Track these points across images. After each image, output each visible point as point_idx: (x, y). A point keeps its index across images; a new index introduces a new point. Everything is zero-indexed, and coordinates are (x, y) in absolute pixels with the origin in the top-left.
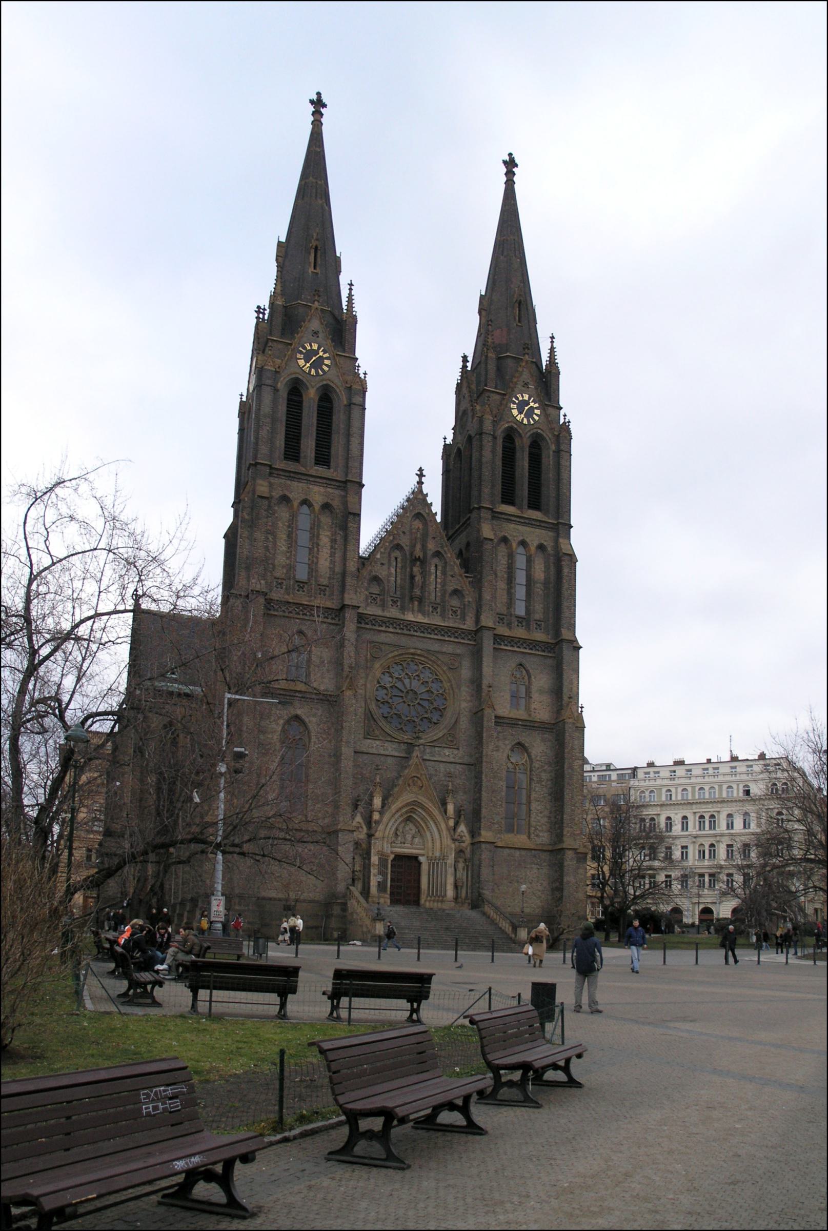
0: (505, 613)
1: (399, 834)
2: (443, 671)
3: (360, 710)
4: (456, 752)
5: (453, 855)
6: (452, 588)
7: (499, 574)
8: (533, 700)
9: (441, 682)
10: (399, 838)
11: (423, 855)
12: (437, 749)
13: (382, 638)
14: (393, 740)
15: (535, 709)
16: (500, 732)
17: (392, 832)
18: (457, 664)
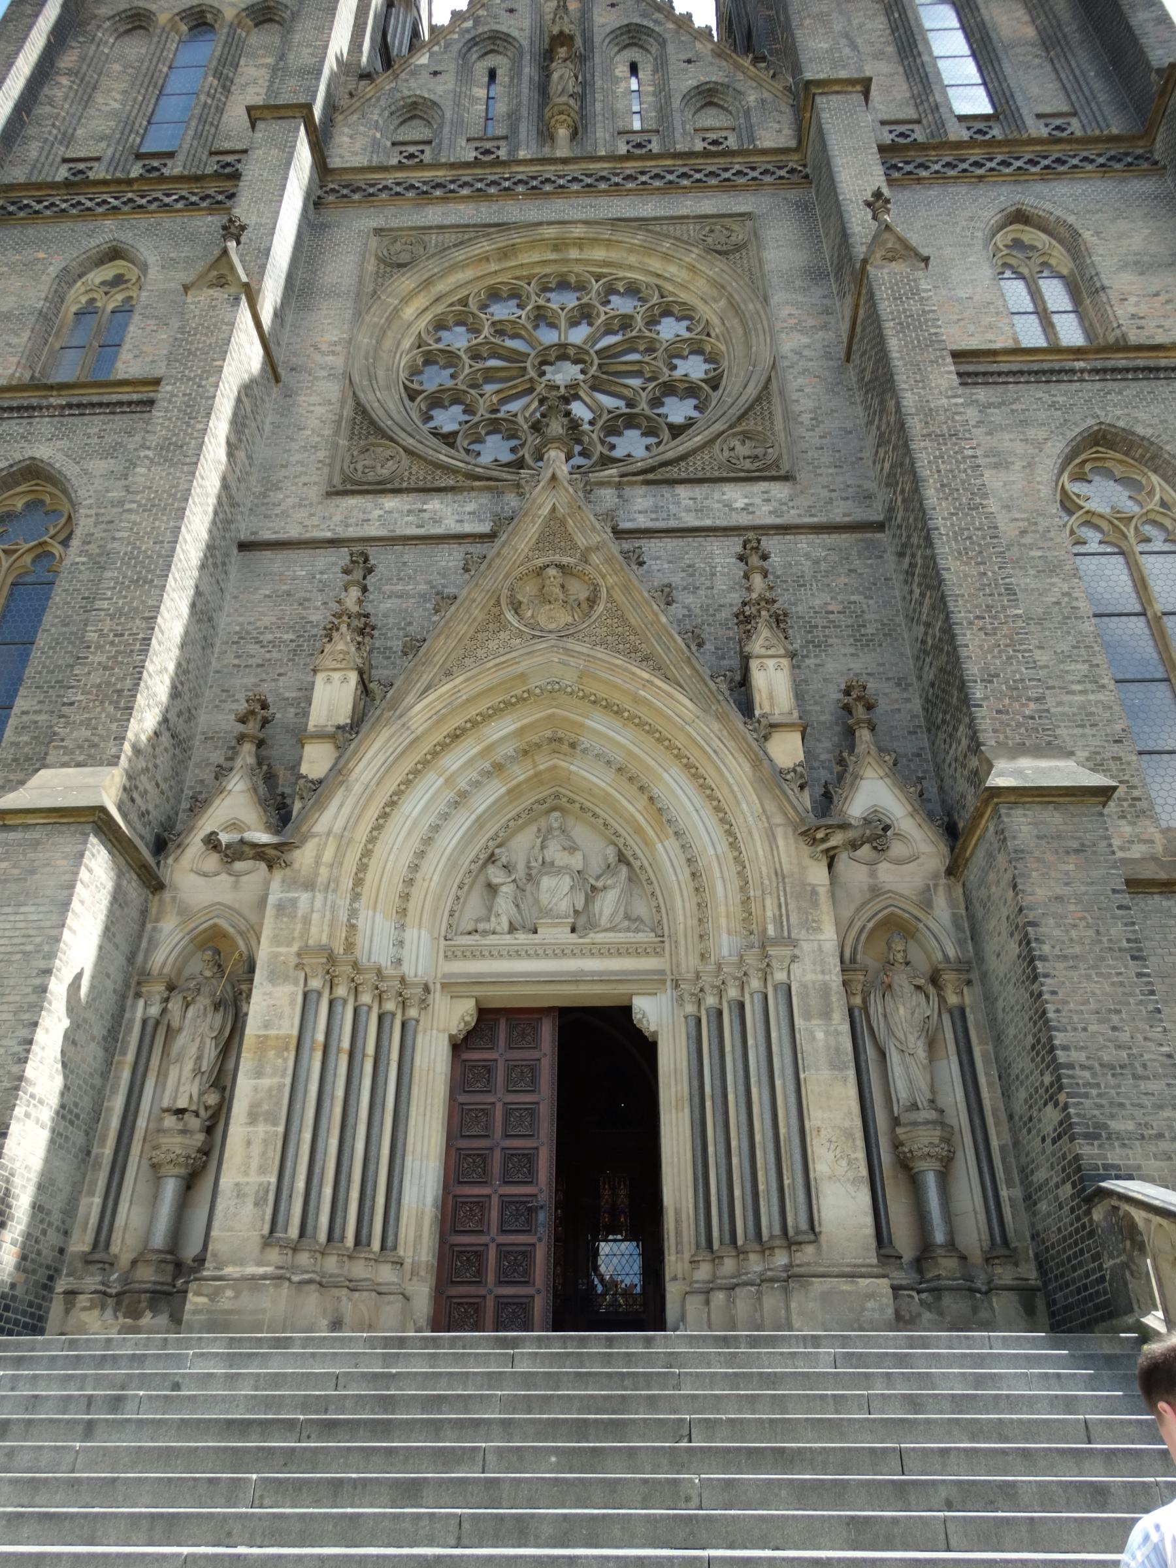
0: (915, 116)
1: (496, 875)
2: (692, 269)
3: (320, 410)
4: (779, 490)
5: (828, 936)
6: (692, 83)
7: (865, 49)
8: (1114, 296)
9: (686, 314)
10: (504, 904)
11: (653, 982)
12: (683, 492)
13: (433, 215)
14: (468, 483)
15: (1133, 316)
16: (990, 405)
17: (434, 869)
18: (739, 235)
